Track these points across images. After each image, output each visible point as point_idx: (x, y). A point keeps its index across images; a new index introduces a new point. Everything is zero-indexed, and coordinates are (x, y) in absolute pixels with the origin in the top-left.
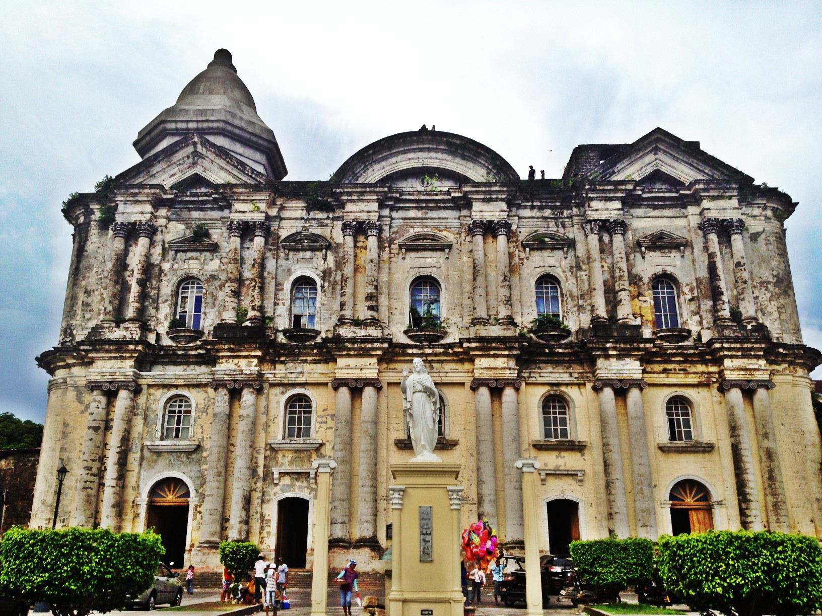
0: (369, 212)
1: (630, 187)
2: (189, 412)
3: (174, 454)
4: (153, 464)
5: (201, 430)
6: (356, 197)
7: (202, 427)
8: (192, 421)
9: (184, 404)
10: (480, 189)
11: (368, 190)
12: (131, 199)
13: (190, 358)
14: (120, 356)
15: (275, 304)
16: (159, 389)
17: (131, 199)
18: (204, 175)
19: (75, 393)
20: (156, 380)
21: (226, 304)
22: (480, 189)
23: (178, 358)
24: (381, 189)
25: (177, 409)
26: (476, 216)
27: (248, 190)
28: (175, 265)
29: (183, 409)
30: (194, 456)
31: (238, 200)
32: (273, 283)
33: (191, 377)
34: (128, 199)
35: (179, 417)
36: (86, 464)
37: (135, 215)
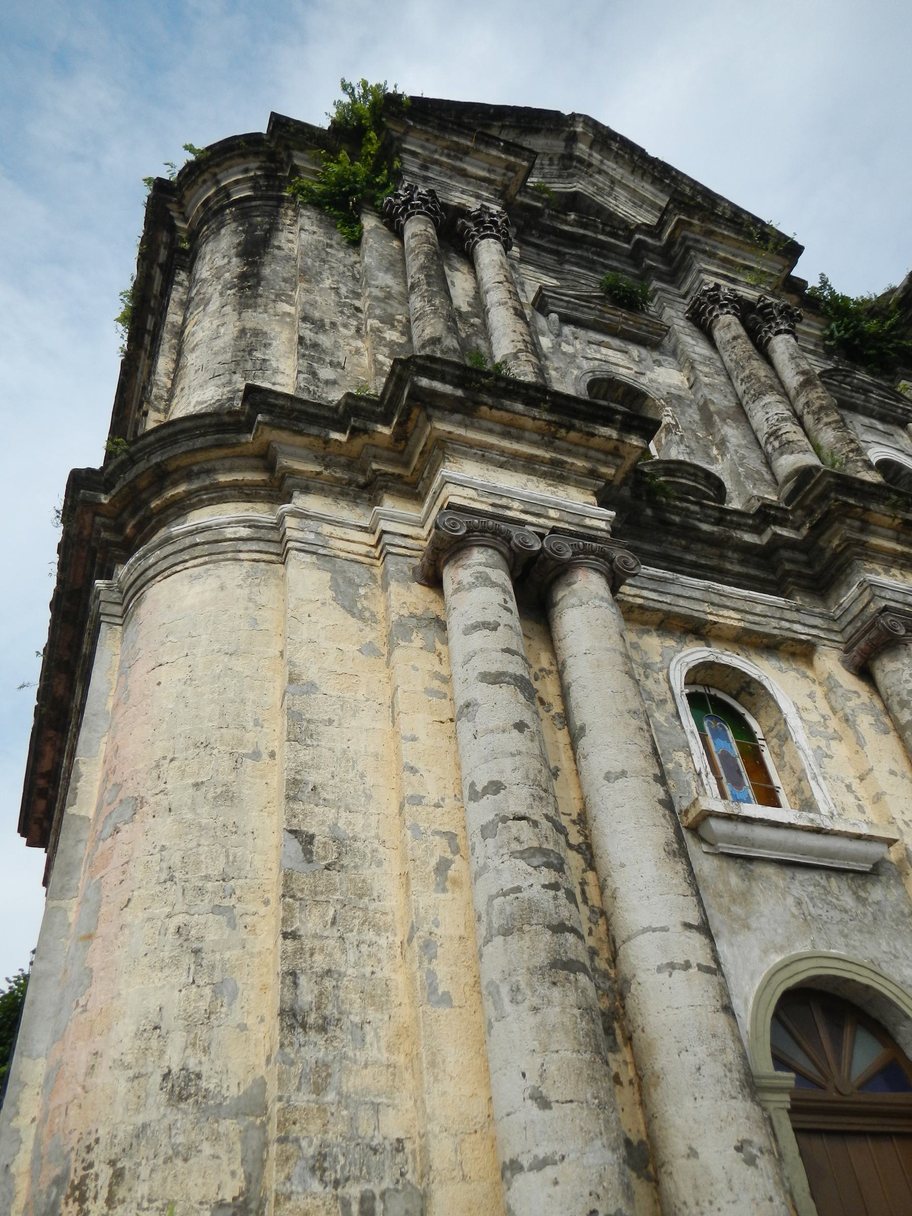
3: (801, 876)
4: (737, 910)
5: (850, 800)
7: (849, 787)
12: (444, 159)
13: (722, 557)
14: (553, 463)
16: (648, 632)
17: (444, 159)
18: (599, 199)
19: (327, 576)
20: (645, 593)
21: (791, 437)
23: (687, 549)
27: (741, 238)
28: (563, 344)
30: (876, 893)
31: (712, 255)
33: (759, 609)
34: (436, 156)
36: (528, 836)
37: (458, 194)
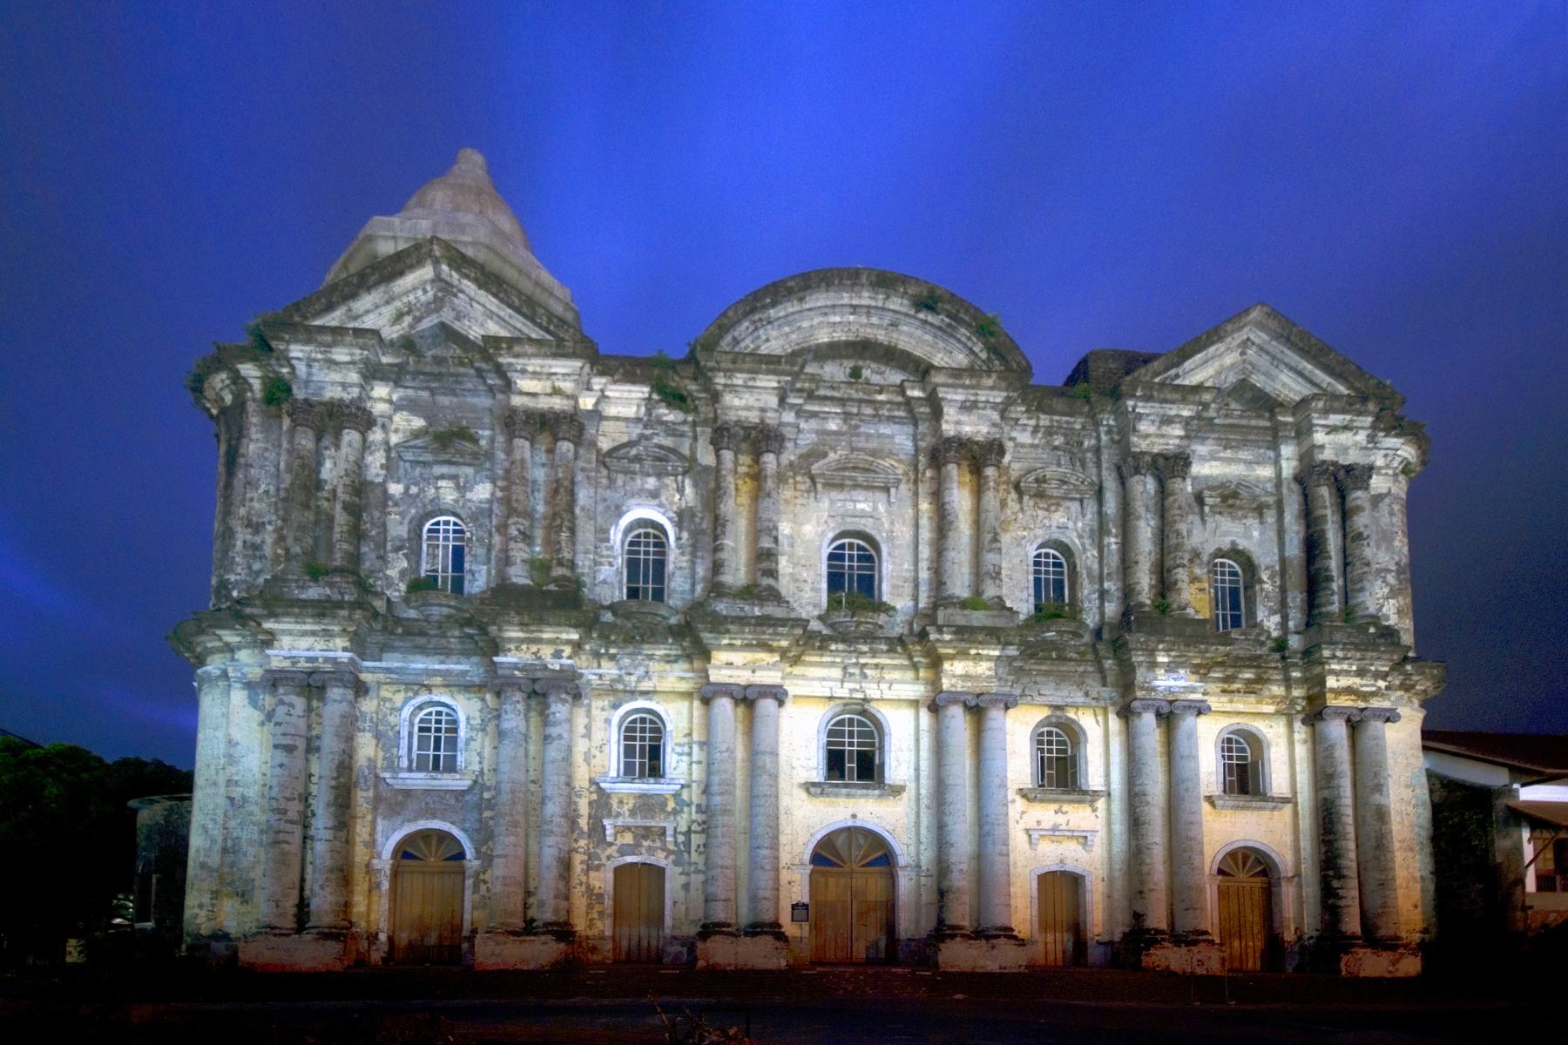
0: (763, 410)
1: (1207, 397)
2: (455, 730)
6: (740, 382)
8: (461, 745)
9: (444, 718)
10: (961, 382)
11: (764, 367)
15: (596, 563)
22: (961, 382)
24: (788, 367)
25: (433, 726)
26: (948, 429)
29: (443, 726)
32: (590, 526)
35: (438, 740)
